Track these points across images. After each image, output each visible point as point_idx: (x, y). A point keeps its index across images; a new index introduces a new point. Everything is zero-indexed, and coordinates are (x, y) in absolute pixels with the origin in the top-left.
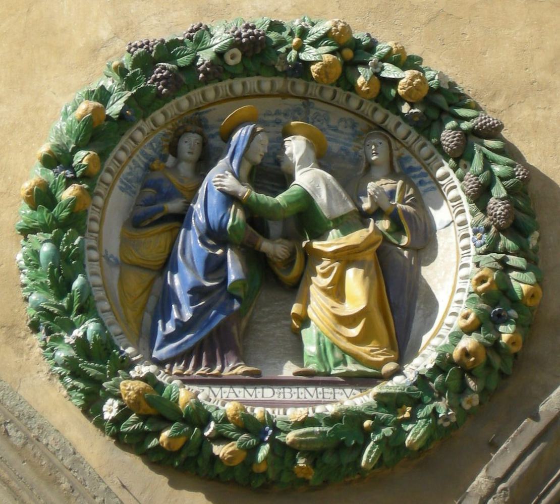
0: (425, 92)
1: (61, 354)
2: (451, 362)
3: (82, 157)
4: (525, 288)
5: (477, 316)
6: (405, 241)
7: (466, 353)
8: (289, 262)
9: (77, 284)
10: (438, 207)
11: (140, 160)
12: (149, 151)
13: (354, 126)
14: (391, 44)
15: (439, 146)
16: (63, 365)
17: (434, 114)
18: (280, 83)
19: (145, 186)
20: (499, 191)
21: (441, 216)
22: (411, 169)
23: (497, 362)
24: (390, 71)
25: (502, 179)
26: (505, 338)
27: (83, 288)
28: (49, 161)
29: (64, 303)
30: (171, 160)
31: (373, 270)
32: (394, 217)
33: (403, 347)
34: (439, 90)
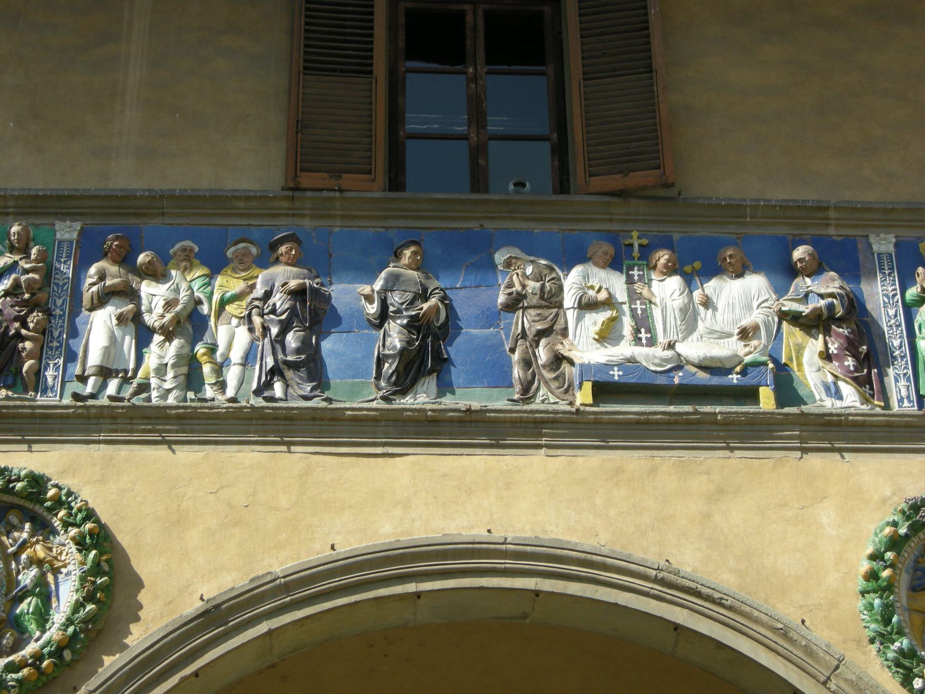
1: (891, 655)
3: (889, 555)
9: (895, 619)
11: (912, 557)
12: (916, 553)
16: (892, 661)
27: (899, 622)
28: (873, 557)
29: (889, 629)
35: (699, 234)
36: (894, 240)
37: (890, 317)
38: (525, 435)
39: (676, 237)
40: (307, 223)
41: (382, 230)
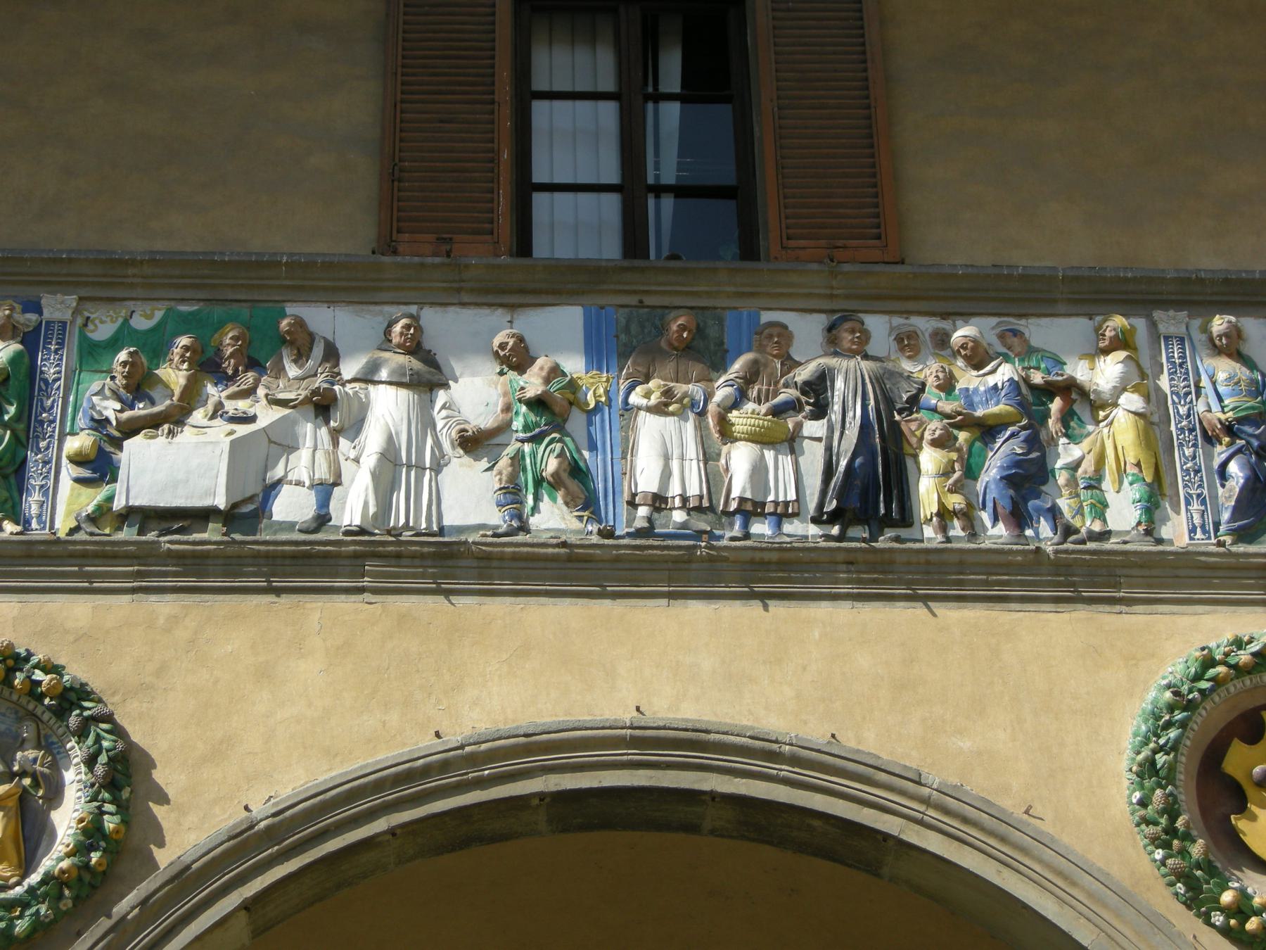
0: (60, 689)
2: (53, 878)
4: (112, 826)
5: (75, 846)
6: (41, 793)
7: (62, 871)
10: (67, 770)
13: (16, 713)
14: (41, 656)
15: (68, 726)
17: (66, 705)
20: (103, 758)
21: (69, 776)
22: (53, 743)
23: (87, 877)
24: (38, 675)
25: (108, 751)
26: (94, 861)
31: (12, 813)
32: (34, 776)
33: (27, 866)
34: (72, 689)
37: (1181, 416)
38: (543, 579)
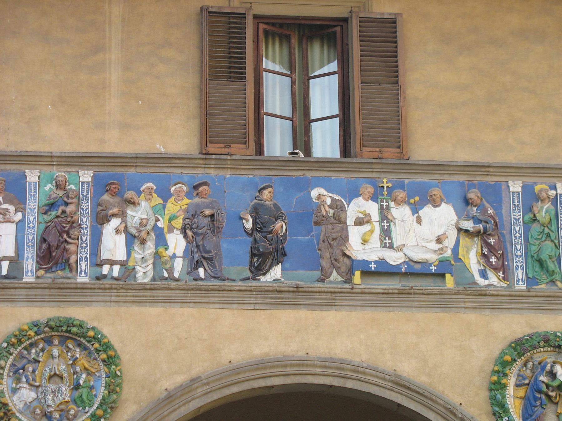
8: (556, 397)
18: (552, 349)
19: (519, 375)
30: (524, 368)
35: (418, 180)
36: (521, 185)
39: (407, 181)
40: (212, 172)
41: (252, 176)
